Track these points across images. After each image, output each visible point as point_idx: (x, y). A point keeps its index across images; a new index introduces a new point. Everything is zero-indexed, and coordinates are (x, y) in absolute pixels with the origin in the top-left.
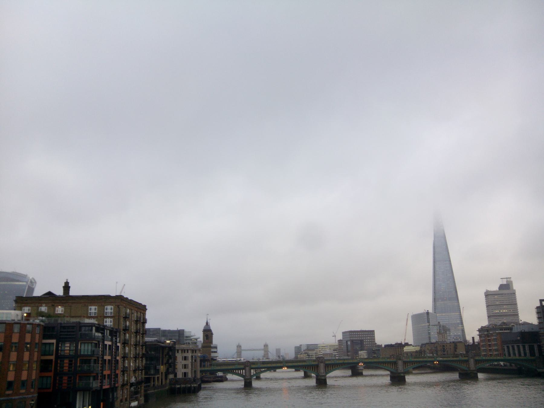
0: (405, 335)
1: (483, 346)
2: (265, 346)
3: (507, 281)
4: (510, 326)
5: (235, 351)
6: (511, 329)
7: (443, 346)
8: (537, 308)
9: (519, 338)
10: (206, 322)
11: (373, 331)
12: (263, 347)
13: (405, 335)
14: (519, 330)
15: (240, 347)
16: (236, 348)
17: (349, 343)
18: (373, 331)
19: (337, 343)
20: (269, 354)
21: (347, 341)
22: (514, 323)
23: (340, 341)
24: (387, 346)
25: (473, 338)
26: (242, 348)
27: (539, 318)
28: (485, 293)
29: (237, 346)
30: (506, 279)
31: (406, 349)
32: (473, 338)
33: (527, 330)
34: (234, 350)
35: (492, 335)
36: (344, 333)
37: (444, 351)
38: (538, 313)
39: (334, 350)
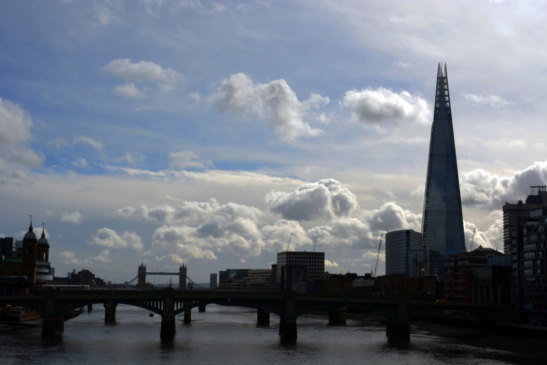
0: (377, 264)
2: (181, 269)
3: (539, 192)
5: (137, 275)
10: (29, 226)
11: (324, 253)
12: (178, 271)
13: (377, 264)
15: (145, 268)
16: (137, 270)
18: (324, 253)
19: (270, 268)
20: (187, 281)
21: (283, 268)
23: (273, 266)
26: (147, 271)
29: (140, 268)
30: (537, 189)
31: (356, 284)
34: (135, 273)
36: (279, 254)
39: (267, 280)
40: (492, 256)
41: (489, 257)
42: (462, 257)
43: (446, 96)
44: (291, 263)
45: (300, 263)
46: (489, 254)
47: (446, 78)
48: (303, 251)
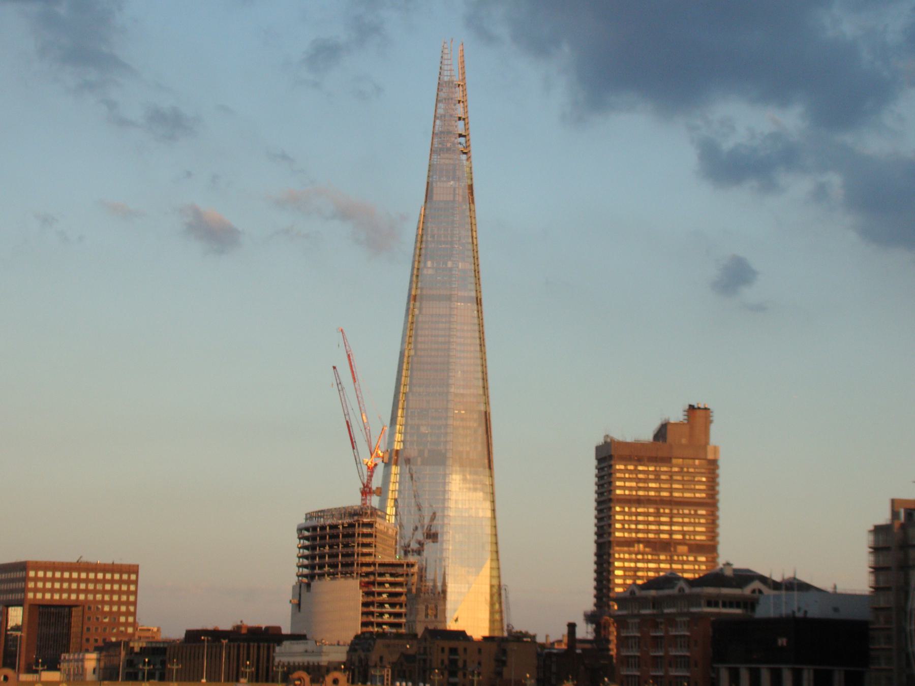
1: (625, 661)
4: (747, 591)
6: (750, 604)
7: (453, 651)
8: (878, 530)
9: (782, 641)
14: (784, 611)
17: (16, 616)
18: (133, 569)
22: (763, 579)
24: (193, 636)
25: (572, 627)
27: (877, 570)
28: (598, 449)
32: (572, 627)
33: (815, 612)
35: (671, 621)
37: (453, 674)
38: (876, 550)
40: (760, 592)
41: (754, 591)
42: (681, 590)
43: (460, 136)
44: (39, 596)
45: (65, 596)
46: (756, 585)
47: (462, 85)
48: (109, 562)
